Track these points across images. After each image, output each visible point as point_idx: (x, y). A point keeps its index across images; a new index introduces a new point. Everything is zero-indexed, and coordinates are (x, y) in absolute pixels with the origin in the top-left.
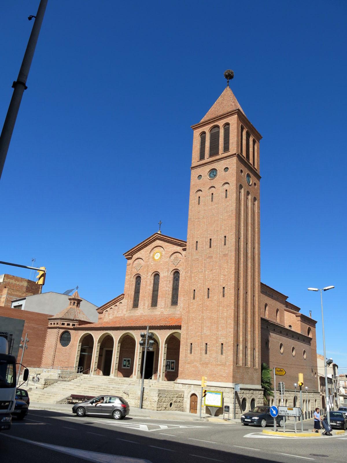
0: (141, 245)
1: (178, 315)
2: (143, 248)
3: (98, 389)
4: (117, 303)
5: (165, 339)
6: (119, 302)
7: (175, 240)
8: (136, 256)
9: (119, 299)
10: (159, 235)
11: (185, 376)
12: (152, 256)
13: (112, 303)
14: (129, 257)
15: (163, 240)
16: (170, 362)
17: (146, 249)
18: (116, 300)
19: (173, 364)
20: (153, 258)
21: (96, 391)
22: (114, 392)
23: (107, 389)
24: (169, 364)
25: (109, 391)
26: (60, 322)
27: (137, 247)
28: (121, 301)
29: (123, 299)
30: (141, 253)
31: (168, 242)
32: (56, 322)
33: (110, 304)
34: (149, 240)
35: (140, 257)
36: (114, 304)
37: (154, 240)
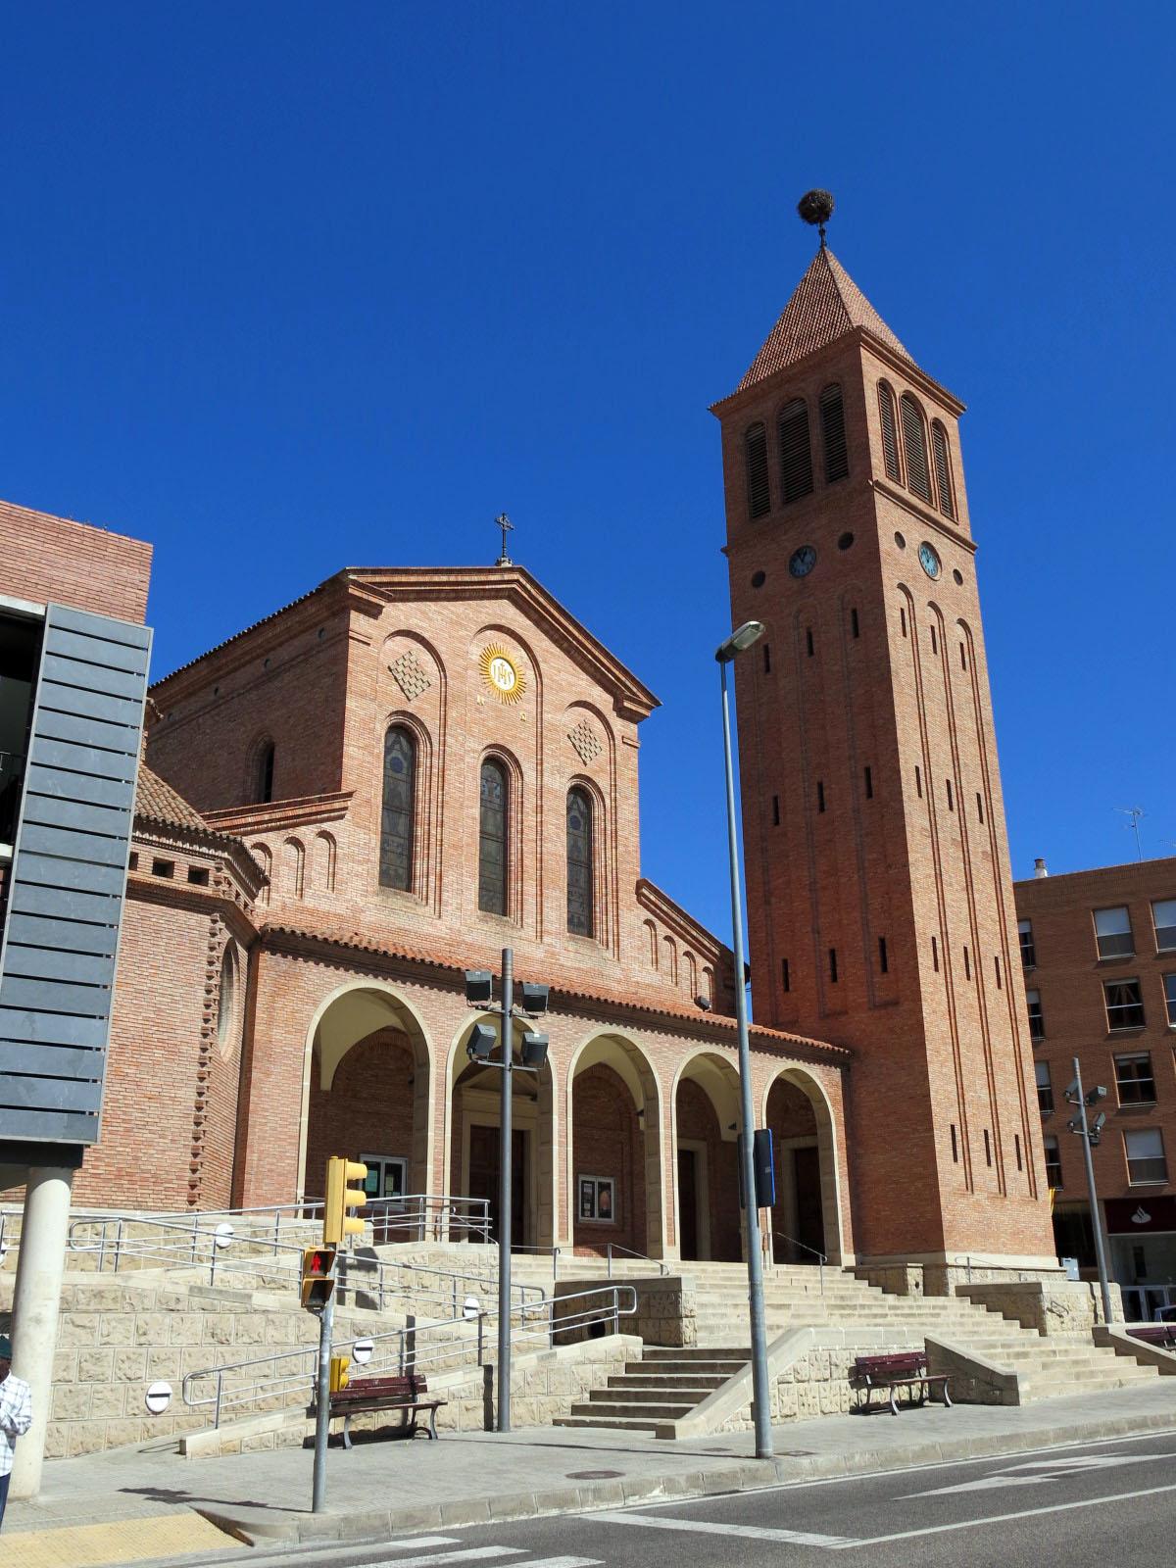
0: (444, 578)
1: (619, 982)
2: (443, 595)
3: (867, 1312)
4: (303, 828)
5: (767, 1093)
6: (314, 828)
7: (597, 654)
8: (402, 618)
9: (323, 808)
10: (528, 586)
11: (961, 1241)
12: (476, 658)
13: (274, 816)
14: (365, 596)
15: (536, 617)
16: (593, 1183)
17: (452, 609)
18: (307, 810)
19: (604, 1194)
20: (484, 668)
21: (889, 1319)
22: (956, 1315)
23: (903, 1307)
24: (590, 1191)
25: (938, 1315)
26: (226, 873)
27: (427, 579)
28: (326, 826)
29: (342, 817)
30: (423, 613)
31: (555, 641)
32: (183, 863)
33: (267, 817)
34: (483, 578)
35: (426, 635)
36: (279, 828)
37: (496, 595)
